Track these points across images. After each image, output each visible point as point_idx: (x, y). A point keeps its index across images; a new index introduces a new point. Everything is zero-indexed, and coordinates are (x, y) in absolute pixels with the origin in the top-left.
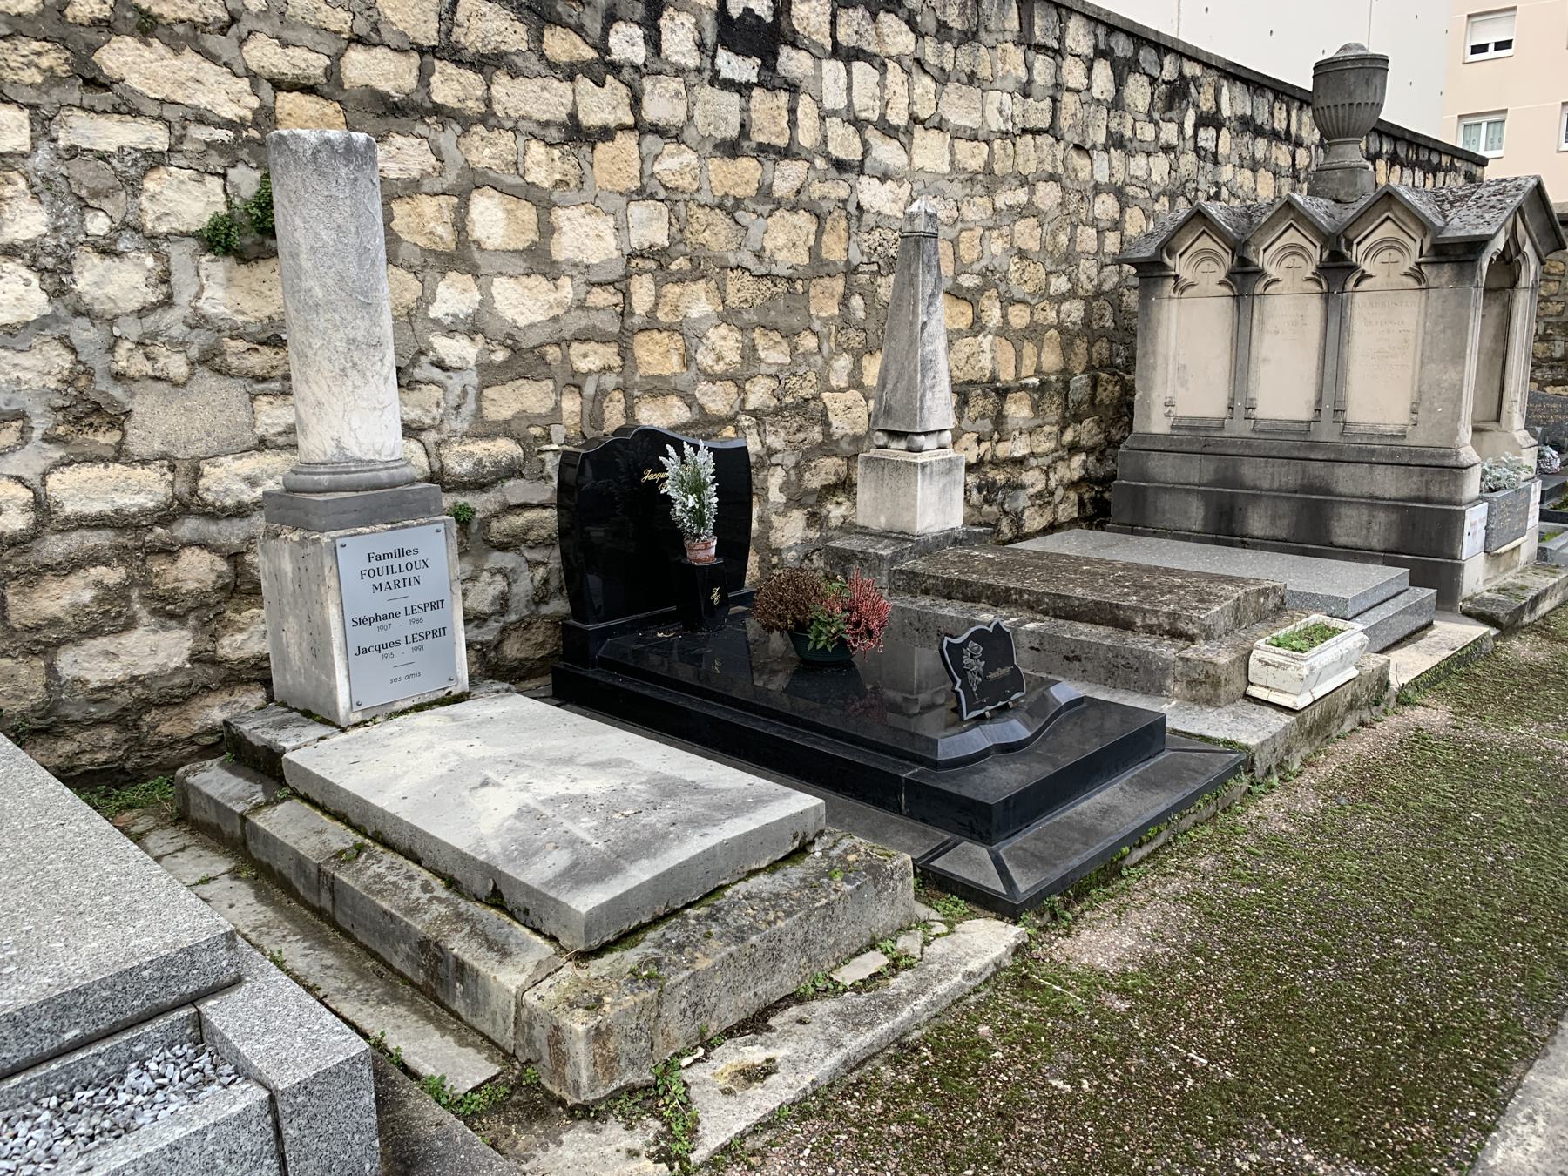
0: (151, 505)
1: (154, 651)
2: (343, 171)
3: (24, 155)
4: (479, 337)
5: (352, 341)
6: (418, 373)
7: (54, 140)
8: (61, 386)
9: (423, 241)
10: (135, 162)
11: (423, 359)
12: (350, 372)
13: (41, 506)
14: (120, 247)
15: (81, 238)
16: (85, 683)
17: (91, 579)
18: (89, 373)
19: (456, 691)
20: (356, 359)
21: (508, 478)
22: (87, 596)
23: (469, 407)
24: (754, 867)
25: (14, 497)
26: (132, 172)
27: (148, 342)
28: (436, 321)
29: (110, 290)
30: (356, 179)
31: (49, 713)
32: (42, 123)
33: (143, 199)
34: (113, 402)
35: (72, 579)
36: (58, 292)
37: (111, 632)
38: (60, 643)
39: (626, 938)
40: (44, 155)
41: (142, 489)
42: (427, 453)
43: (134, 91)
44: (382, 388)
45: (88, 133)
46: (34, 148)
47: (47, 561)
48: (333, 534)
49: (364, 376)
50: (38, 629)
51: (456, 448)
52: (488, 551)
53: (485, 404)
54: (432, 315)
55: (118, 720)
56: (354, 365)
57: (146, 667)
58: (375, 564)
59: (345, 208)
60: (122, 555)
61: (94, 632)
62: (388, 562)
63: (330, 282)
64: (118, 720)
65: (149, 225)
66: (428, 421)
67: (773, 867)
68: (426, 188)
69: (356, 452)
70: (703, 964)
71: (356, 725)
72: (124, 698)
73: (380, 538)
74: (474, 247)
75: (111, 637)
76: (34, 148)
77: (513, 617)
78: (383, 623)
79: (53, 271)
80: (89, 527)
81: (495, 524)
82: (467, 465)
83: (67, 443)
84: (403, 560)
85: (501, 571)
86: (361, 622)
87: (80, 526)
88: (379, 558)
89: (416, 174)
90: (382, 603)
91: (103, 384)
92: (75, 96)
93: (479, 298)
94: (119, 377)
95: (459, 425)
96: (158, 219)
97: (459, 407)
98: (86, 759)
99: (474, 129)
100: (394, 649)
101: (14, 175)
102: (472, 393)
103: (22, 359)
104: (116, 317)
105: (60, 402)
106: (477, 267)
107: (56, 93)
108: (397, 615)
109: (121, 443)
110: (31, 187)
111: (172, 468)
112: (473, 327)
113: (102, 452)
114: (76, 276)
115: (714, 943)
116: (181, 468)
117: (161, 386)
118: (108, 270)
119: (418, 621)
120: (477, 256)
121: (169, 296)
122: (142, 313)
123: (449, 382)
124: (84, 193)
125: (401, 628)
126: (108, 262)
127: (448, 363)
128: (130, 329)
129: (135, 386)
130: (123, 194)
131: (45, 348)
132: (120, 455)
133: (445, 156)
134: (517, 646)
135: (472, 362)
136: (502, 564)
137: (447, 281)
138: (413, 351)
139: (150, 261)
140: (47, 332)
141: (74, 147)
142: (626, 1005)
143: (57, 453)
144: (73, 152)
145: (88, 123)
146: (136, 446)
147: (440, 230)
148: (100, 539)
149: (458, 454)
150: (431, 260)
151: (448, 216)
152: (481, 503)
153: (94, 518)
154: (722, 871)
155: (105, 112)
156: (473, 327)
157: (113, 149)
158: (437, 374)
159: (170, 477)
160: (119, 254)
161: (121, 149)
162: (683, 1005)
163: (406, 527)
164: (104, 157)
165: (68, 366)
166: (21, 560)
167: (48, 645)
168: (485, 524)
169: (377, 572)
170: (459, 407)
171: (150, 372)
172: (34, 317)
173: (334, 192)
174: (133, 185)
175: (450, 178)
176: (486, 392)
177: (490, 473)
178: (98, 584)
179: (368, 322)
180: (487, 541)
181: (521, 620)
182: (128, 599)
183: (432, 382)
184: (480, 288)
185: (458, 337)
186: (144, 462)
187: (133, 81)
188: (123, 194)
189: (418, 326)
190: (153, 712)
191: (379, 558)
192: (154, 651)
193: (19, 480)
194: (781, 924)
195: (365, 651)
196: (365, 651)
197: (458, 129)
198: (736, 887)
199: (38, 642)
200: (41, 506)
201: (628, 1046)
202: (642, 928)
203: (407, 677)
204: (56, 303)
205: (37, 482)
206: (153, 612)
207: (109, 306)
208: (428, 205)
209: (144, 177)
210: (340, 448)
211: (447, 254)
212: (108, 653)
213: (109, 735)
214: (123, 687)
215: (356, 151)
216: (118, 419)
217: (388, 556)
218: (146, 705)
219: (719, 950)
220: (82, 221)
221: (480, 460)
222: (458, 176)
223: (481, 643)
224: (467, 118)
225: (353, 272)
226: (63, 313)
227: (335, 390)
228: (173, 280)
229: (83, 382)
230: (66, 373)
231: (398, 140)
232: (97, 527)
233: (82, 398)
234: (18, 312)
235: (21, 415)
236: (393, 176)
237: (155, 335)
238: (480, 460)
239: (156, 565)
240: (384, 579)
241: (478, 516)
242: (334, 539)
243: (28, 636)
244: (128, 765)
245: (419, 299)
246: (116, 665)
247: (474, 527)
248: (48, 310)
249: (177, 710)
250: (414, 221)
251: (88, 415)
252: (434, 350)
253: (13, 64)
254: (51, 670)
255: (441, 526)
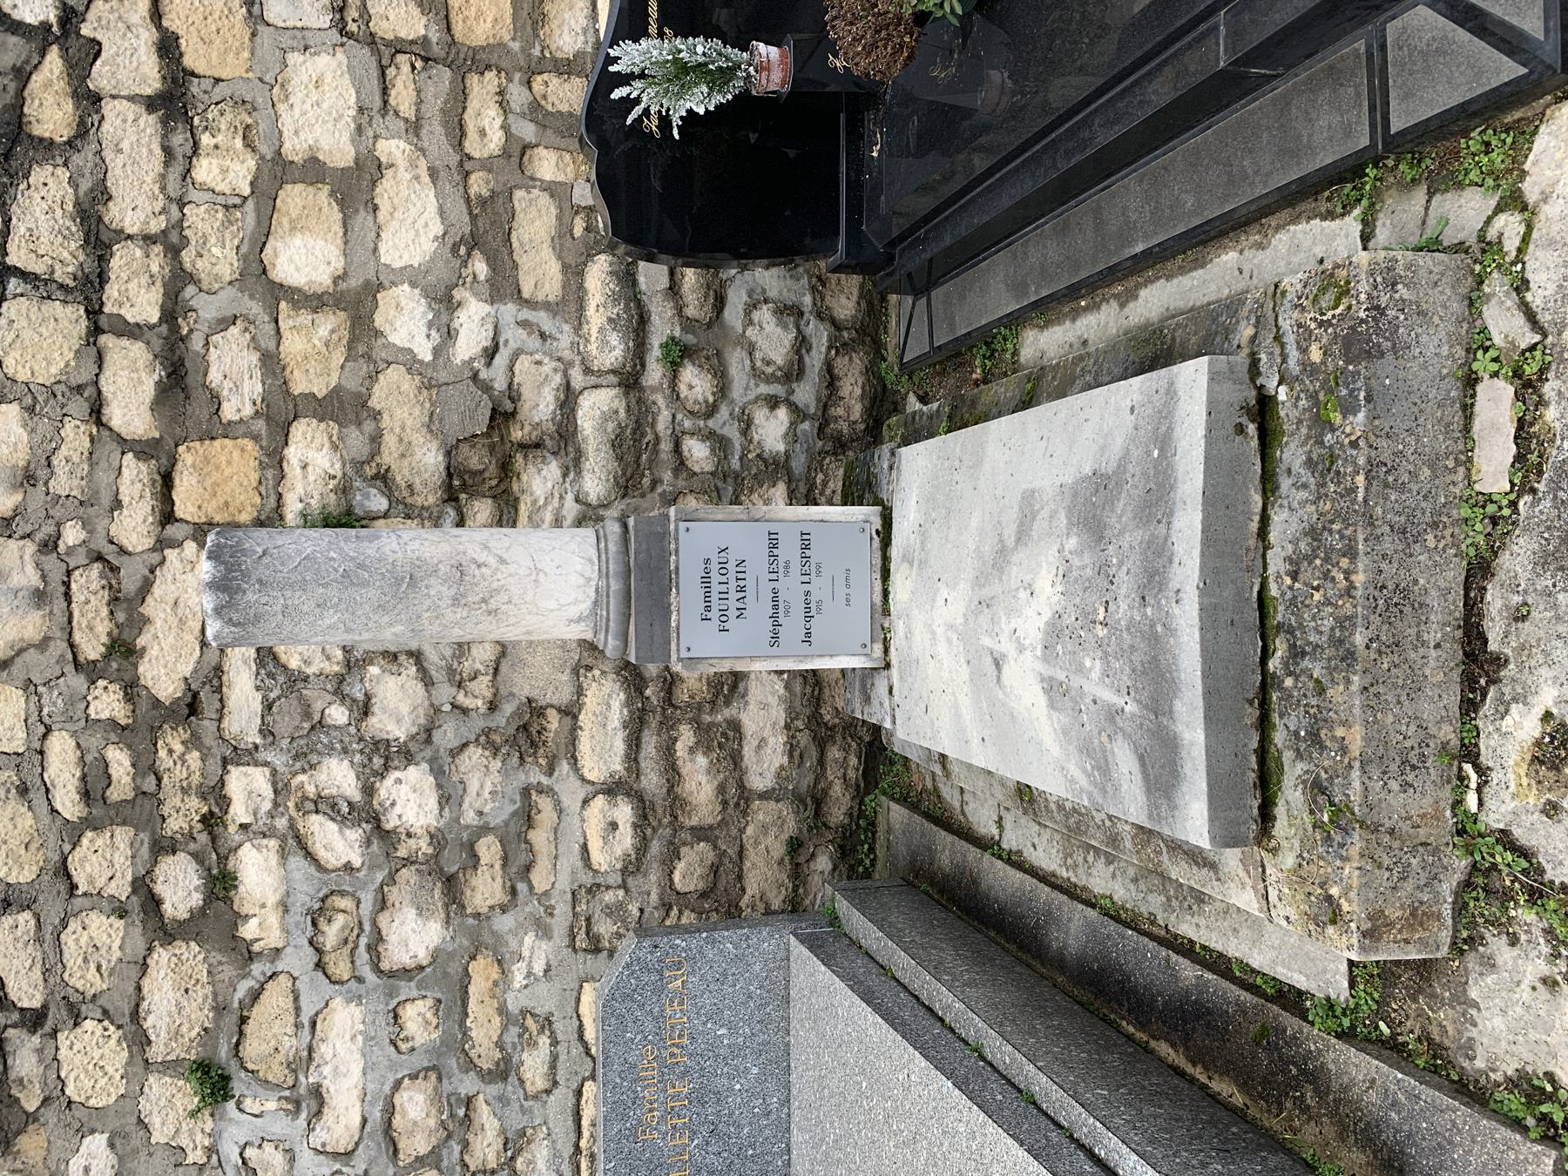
0: (622, 696)
1: (765, 706)
2: (251, 597)
3: (274, 772)
4: (458, 294)
5: (456, 601)
6: (500, 385)
7: (256, 747)
8: (500, 757)
9: (338, 357)
10: (271, 675)
11: (483, 375)
12: (493, 604)
13: (611, 789)
14: (360, 696)
15: (352, 730)
16: (782, 768)
17: (687, 757)
18: (487, 732)
19: (877, 523)
20: (477, 599)
21: (635, 283)
22: (702, 761)
23: (543, 319)
24: (1254, 526)
25: (602, 811)
26: (281, 679)
27: (458, 677)
28: (437, 352)
29: (405, 709)
30: (260, 581)
31: (802, 801)
32: (240, 755)
33: (309, 671)
34: (517, 713)
35: (684, 772)
36: (408, 757)
37: (740, 745)
38: (741, 786)
39: (1267, 783)
40: (269, 756)
41: (605, 705)
42: (596, 387)
43: (195, 671)
44: (512, 568)
45: (245, 717)
46: (266, 764)
47: (664, 790)
48: (674, 657)
49: (497, 591)
50: (725, 803)
51: (593, 348)
52: (723, 326)
53: (540, 297)
54: (428, 358)
55: (822, 745)
56: (484, 601)
57: (779, 714)
58: (714, 614)
59: (296, 598)
60: (668, 726)
61: (736, 758)
62: (715, 596)
63: (386, 619)
64: (822, 745)
65: (336, 668)
66: (558, 379)
67: (1268, 483)
68: (272, 345)
69: (585, 606)
70: (1356, 738)
71: (886, 651)
72: (804, 739)
73: (686, 601)
74: (343, 286)
75: (744, 743)
76: (266, 764)
77: (807, 300)
78: (781, 610)
79: (387, 758)
80: (637, 752)
81: (691, 312)
82: (614, 339)
83: (554, 757)
84: (715, 578)
85: (748, 313)
86: (775, 637)
87: (636, 760)
88: (708, 608)
89: (254, 358)
90: (759, 610)
91: (500, 720)
92: (208, 726)
93: (406, 287)
94: (493, 707)
95: (565, 337)
96: (328, 658)
97: (543, 335)
98: (851, 774)
99: (188, 266)
100: (813, 599)
101: (294, 782)
102: (526, 314)
103: (473, 786)
104: (432, 705)
105: (515, 760)
106: (367, 283)
107: (209, 740)
108: (775, 592)
109: (559, 710)
110: (304, 771)
111: (589, 668)
112: (444, 302)
113: (567, 728)
114: (391, 737)
115: (1335, 693)
116: (590, 661)
117: (504, 668)
118: (384, 711)
119: (787, 567)
120: (354, 282)
121: (410, 654)
122: (427, 681)
123: (512, 345)
124: (307, 725)
125: (791, 588)
126: (375, 709)
127: (487, 343)
128: (444, 693)
129: (503, 691)
130: (304, 692)
131: (462, 769)
132: (570, 713)
133: (229, 313)
134: (843, 300)
135: (487, 308)
136: (741, 308)
137: (386, 329)
138: (473, 388)
139: (374, 670)
140: (446, 768)
141: (260, 731)
142: (1355, 882)
143: (564, 767)
144: (266, 731)
145: (234, 716)
146: (564, 695)
147: (323, 331)
148: (650, 744)
149: (601, 349)
150: (361, 349)
151: (305, 317)
152: (662, 327)
153: (629, 747)
154: (1239, 593)
155: (221, 700)
156: (444, 302)
157: (259, 696)
158: (501, 360)
159: (597, 672)
160: (368, 697)
161: (258, 688)
162: (1394, 785)
163: (677, 568)
164: (268, 706)
165: (480, 751)
166: (660, 811)
167: (740, 797)
168: (688, 324)
169: (723, 612)
170: (543, 335)
171: (489, 678)
172: (432, 779)
173: (278, 608)
174: (296, 680)
175: (255, 308)
176: (526, 295)
177: (627, 309)
178: (692, 750)
179: (432, 581)
180: (709, 325)
181: (813, 289)
182: (711, 725)
183: (511, 369)
184: (394, 284)
185: (456, 324)
186: (580, 692)
187: (186, 669)
188: (304, 692)
189: (443, 376)
190: (823, 711)
191: (708, 608)
192: (765, 706)
193: (586, 802)
194: (1359, 579)
195: (808, 634)
196: (808, 634)
197: (190, 290)
198: (1271, 570)
199: (737, 805)
200: (611, 789)
201: (1409, 886)
202: (1263, 752)
203: (848, 586)
204: (418, 757)
205: (590, 788)
206: (727, 703)
207: (421, 712)
208: (293, 345)
209: (285, 667)
210: (580, 620)
211: (353, 327)
212: (759, 747)
213: (834, 753)
214: (793, 737)
215: (224, 578)
216: (535, 710)
217: (707, 596)
218: (815, 719)
219: (1346, 696)
220: (336, 727)
221: (610, 320)
222: (252, 297)
223: (829, 348)
224: (174, 276)
225: (372, 593)
226: (428, 753)
227: (512, 620)
228: (393, 649)
229: (497, 739)
230: (487, 753)
231: (214, 377)
232: (638, 746)
233: (512, 742)
234: (428, 792)
235: (526, 792)
236: (259, 388)
237: (451, 671)
238: (610, 320)
239: (682, 696)
240: (733, 604)
241: (677, 334)
242: (680, 659)
243: (730, 811)
244: (867, 739)
245: (409, 371)
246: (772, 740)
247: (690, 339)
248: (425, 766)
249: (826, 691)
250: (313, 366)
251: (529, 736)
252: (472, 360)
253: (185, 775)
254: (765, 796)
255: (683, 525)
